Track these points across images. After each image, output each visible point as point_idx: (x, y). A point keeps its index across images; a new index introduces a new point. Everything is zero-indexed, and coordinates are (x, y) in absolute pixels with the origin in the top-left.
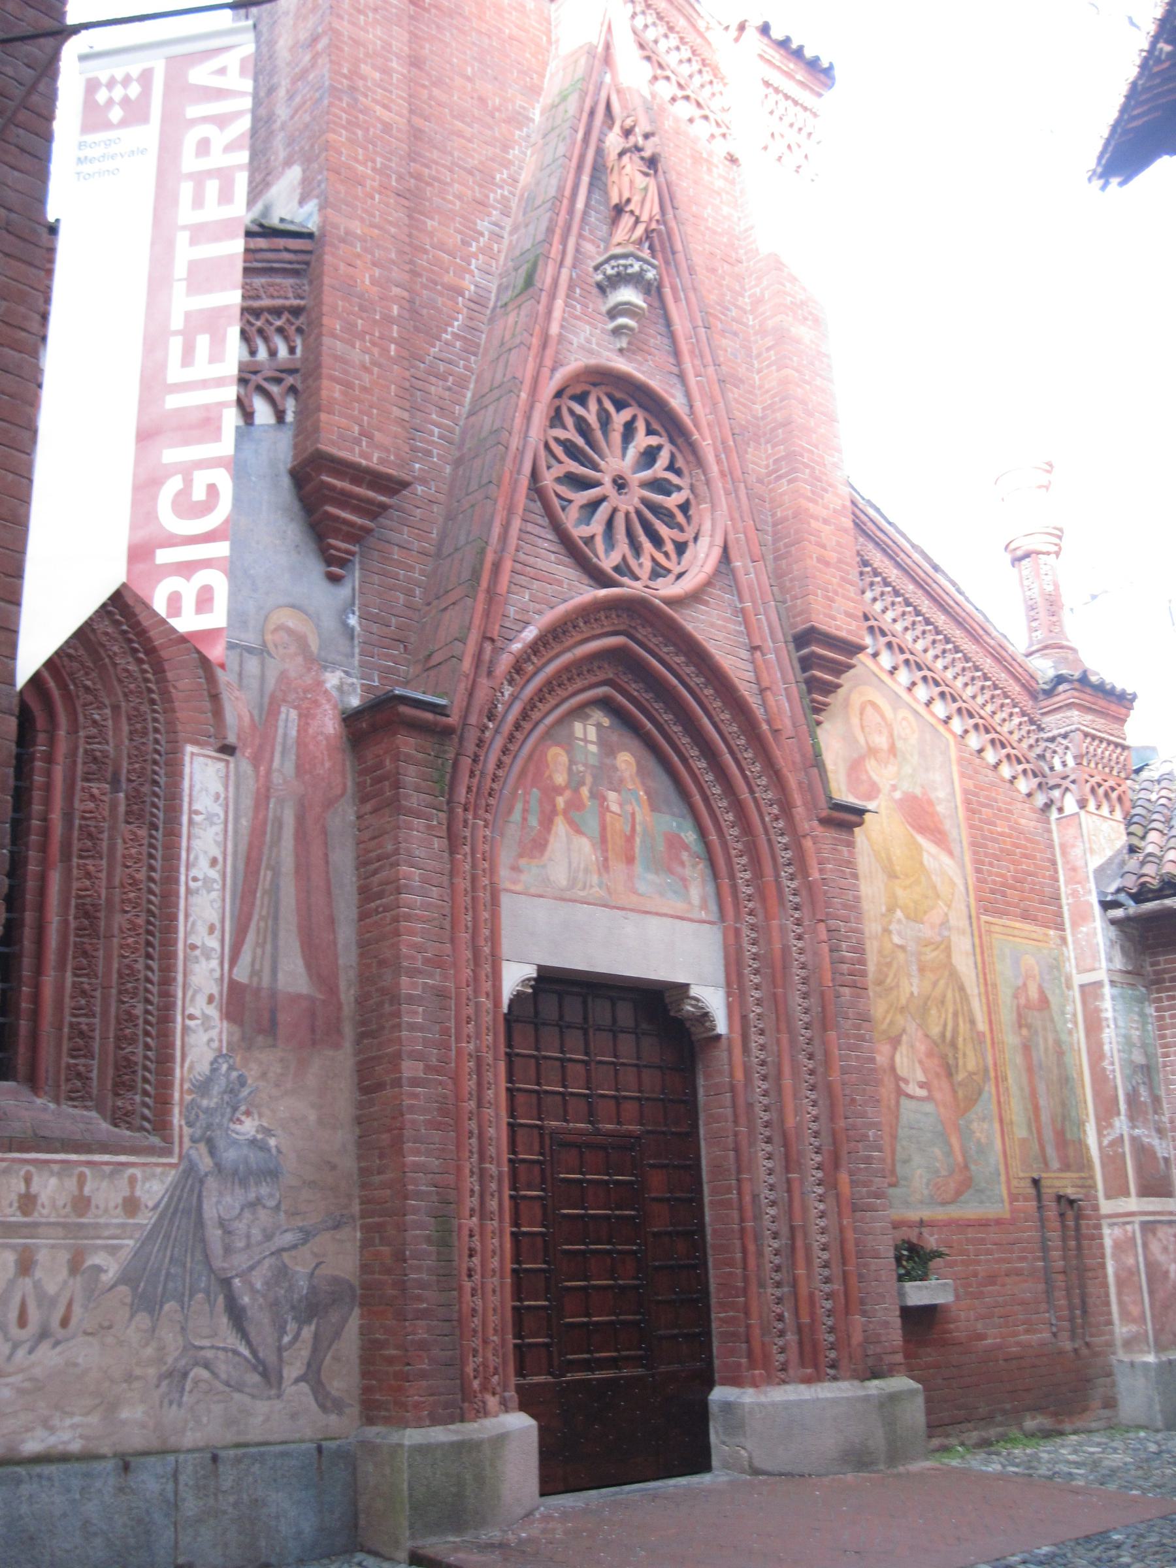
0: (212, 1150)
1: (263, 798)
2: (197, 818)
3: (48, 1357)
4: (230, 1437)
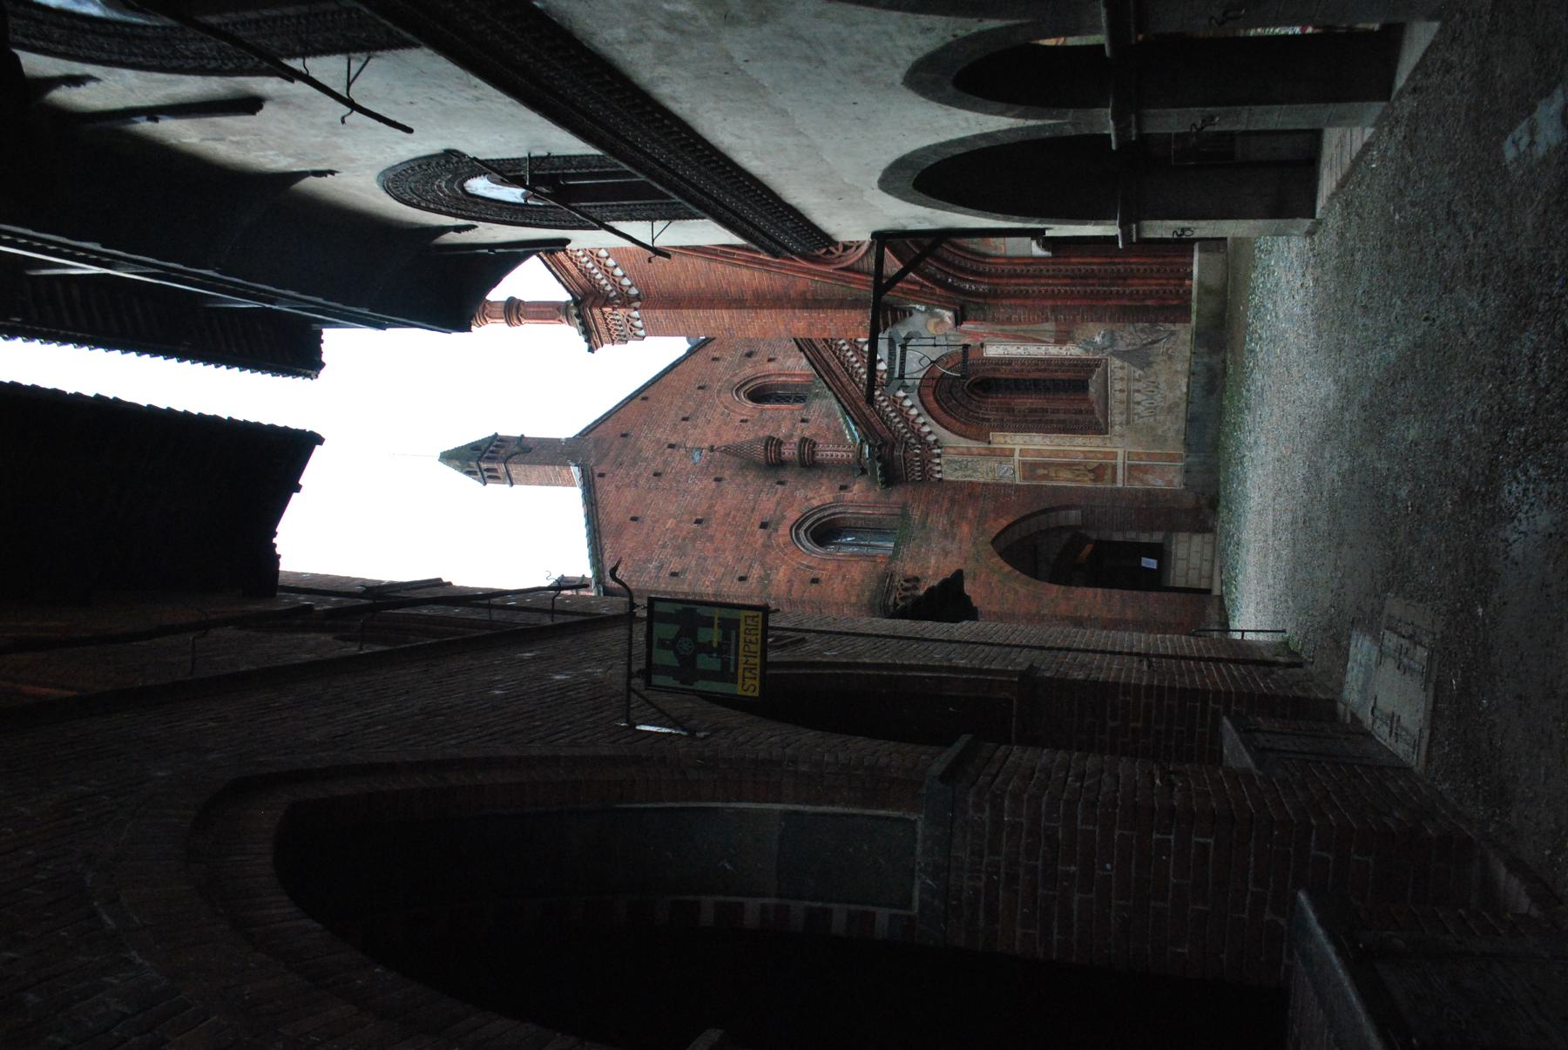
0: (1106, 348)
1: (997, 336)
3: (1162, 386)
4: (1189, 344)
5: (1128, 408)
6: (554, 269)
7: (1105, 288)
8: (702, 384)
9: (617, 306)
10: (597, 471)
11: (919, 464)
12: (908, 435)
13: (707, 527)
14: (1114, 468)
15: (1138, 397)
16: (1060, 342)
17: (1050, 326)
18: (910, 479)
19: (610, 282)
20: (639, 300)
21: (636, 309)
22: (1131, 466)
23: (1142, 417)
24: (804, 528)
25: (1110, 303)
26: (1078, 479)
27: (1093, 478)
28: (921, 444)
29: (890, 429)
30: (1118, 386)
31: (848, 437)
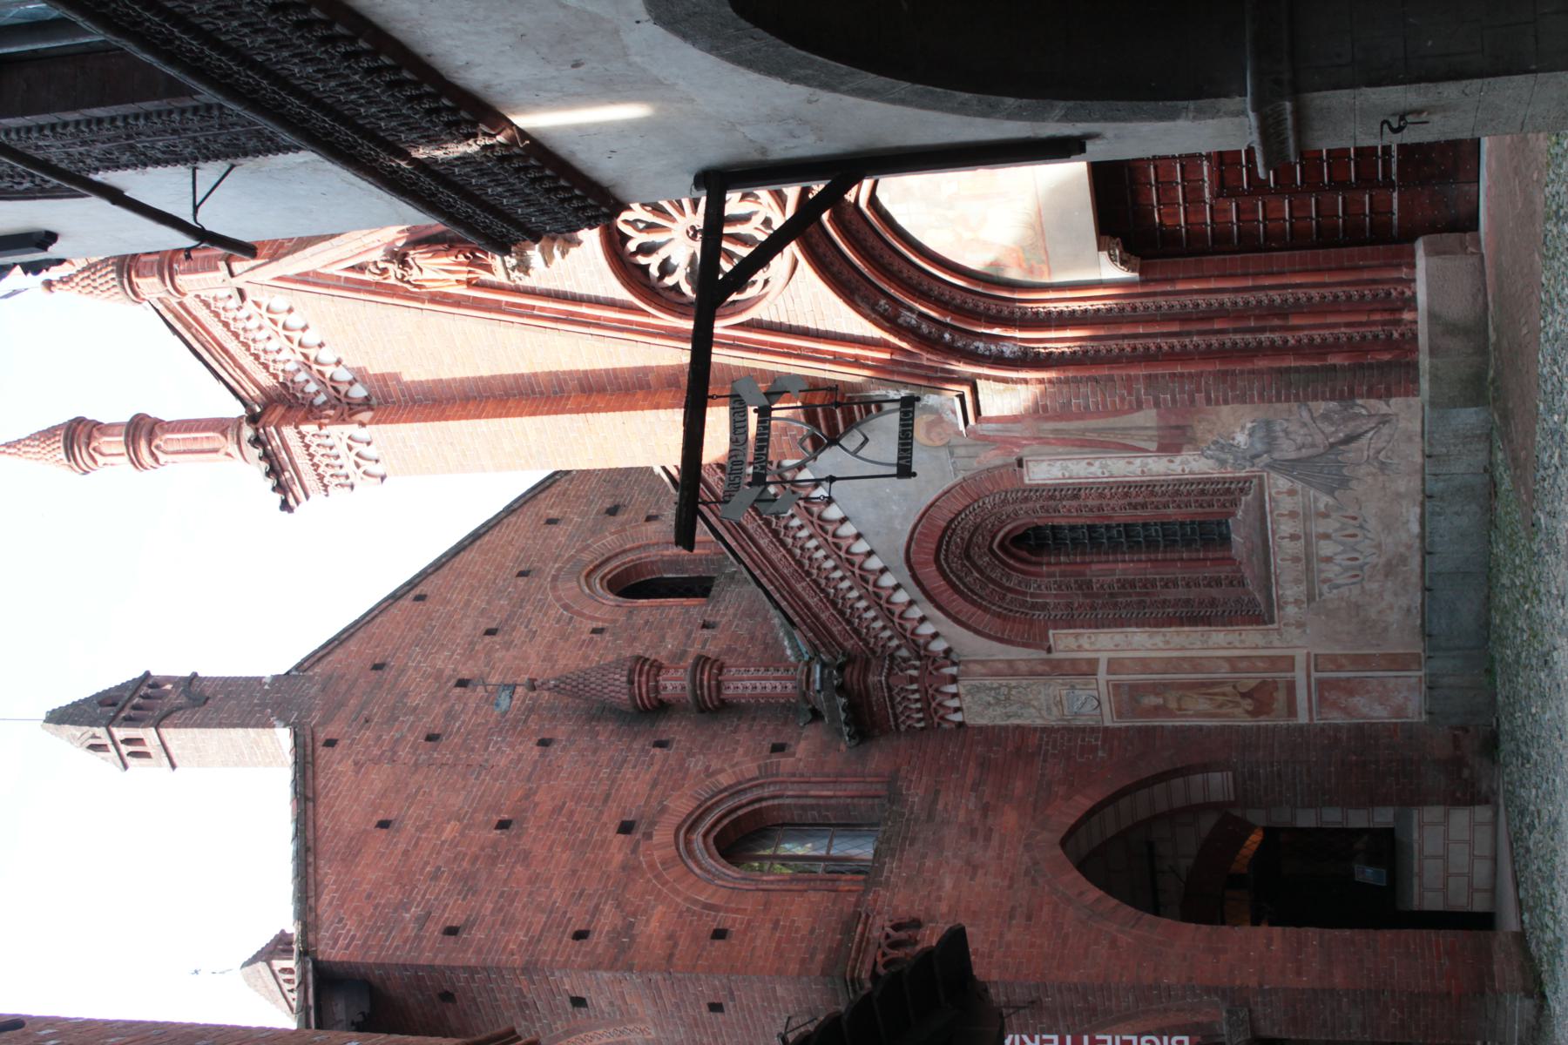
2: (1067, 475)
3: (1372, 523)
4: (1418, 439)
5: (1308, 569)
6: (206, 356)
7: (1248, 337)
8: (523, 567)
9: (327, 421)
10: (322, 736)
11: (917, 696)
12: (895, 643)
13: (519, 837)
14: (1291, 687)
15: (1326, 548)
16: (1170, 446)
17: (1147, 417)
18: (903, 728)
19: (311, 375)
20: (370, 408)
21: (362, 424)
22: (1321, 683)
23: (1338, 587)
24: (702, 830)
25: (1261, 364)
26: (1224, 710)
27: (1250, 708)
28: (919, 658)
29: (856, 631)
30: (1286, 527)
31: (789, 652)
